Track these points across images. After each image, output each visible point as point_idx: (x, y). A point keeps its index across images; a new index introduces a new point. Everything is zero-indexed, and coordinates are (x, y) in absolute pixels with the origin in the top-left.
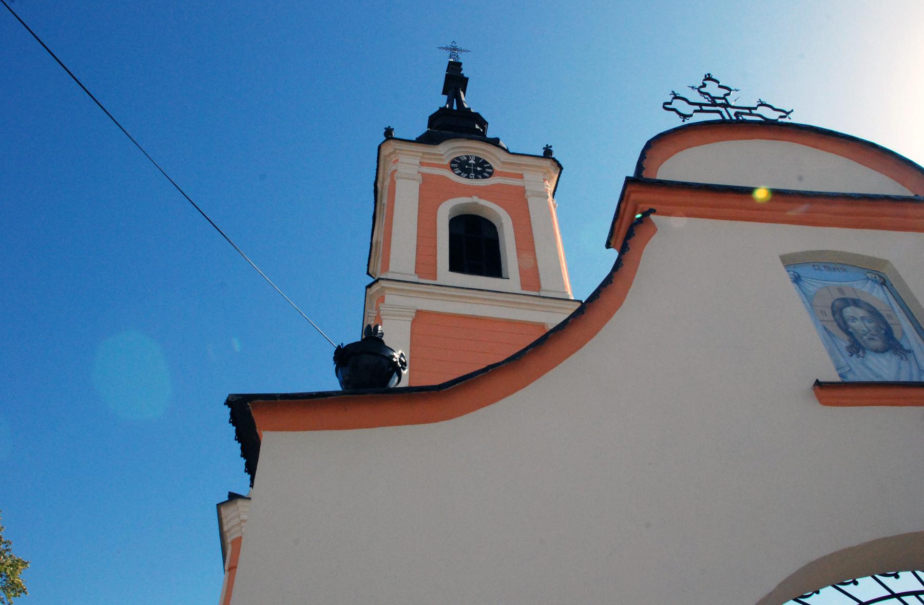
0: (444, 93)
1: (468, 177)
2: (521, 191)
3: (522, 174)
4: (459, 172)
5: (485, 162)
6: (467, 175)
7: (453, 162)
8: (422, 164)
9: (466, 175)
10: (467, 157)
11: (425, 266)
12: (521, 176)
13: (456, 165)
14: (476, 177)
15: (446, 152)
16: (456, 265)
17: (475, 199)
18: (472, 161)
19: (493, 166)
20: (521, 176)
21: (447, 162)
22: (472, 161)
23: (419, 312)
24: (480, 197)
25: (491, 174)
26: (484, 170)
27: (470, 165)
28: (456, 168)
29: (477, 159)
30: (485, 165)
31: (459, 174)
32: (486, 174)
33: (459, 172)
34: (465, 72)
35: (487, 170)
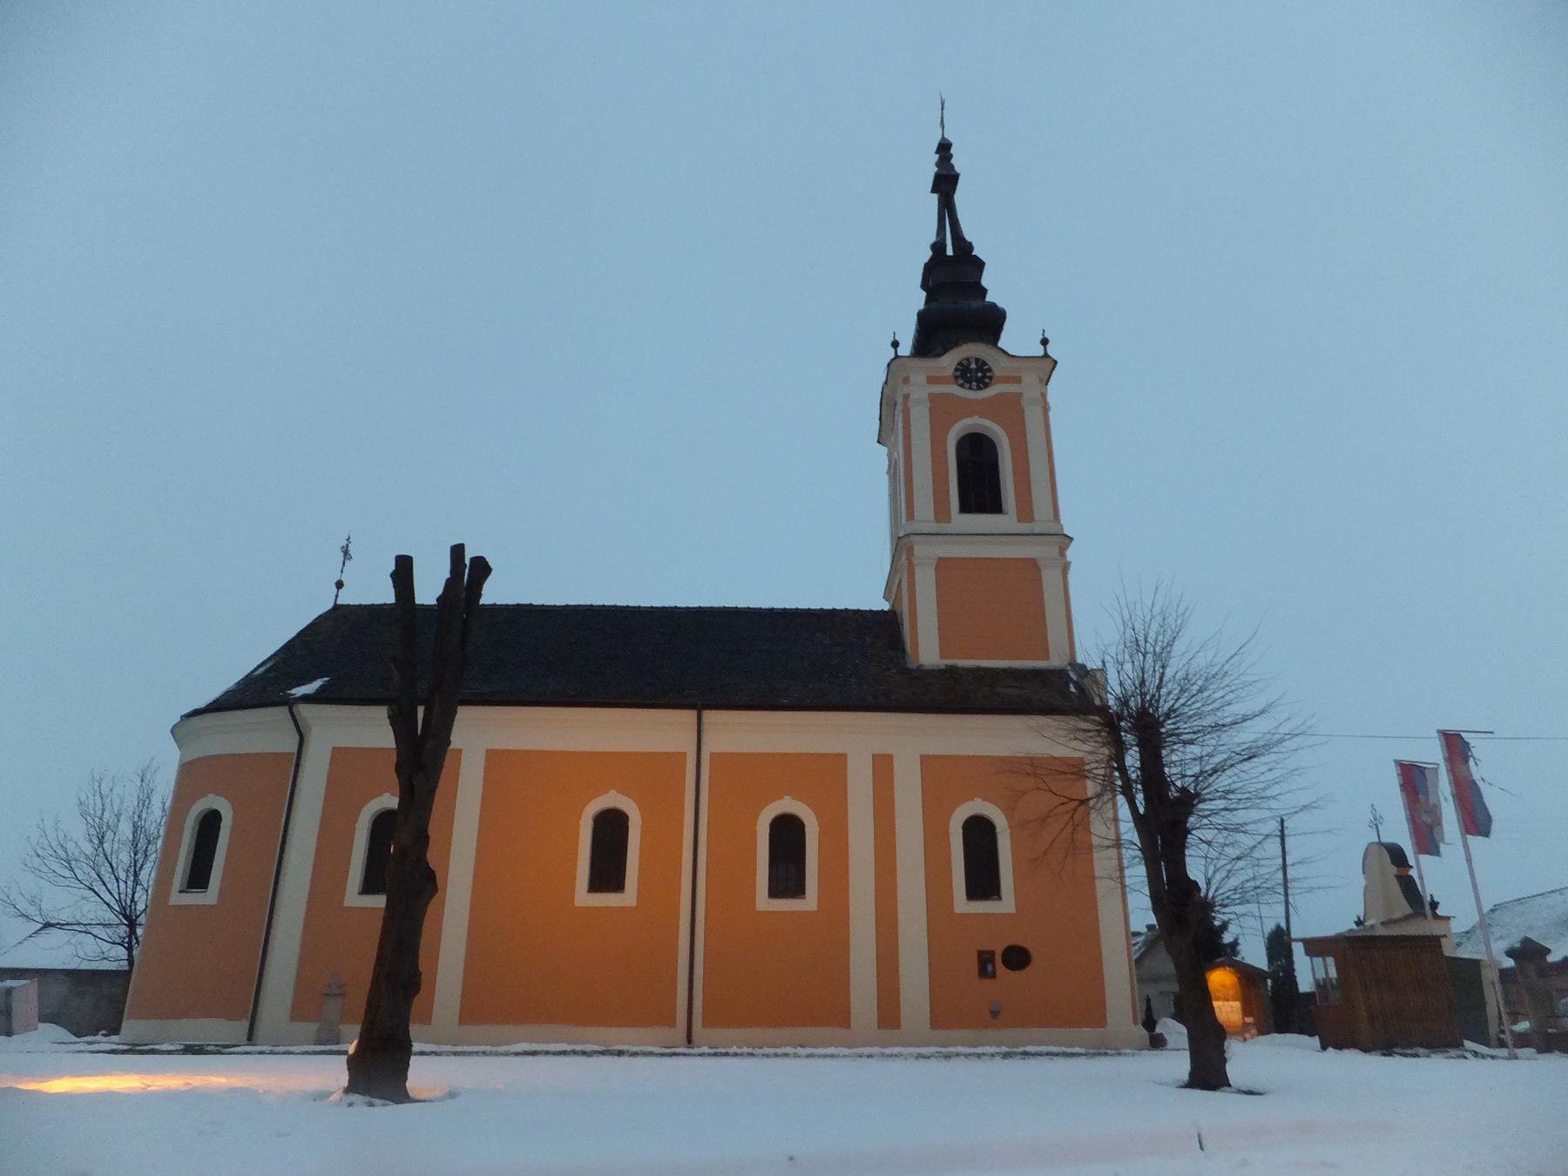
0: (933, 191)
1: (970, 388)
2: (1019, 396)
4: (961, 382)
7: (956, 370)
9: (967, 385)
10: (968, 359)
11: (942, 513)
13: (958, 373)
14: (979, 388)
16: (965, 508)
18: (973, 366)
20: (1017, 380)
21: (950, 372)
22: (973, 366)
23: (940, 559)
26: (984, 376)
27: (970, 371)
29: (977, 360)
30: (986, 367)
31: (962, 386)
32: (987, 380)
34: (957, 162)
35: (988, 374)
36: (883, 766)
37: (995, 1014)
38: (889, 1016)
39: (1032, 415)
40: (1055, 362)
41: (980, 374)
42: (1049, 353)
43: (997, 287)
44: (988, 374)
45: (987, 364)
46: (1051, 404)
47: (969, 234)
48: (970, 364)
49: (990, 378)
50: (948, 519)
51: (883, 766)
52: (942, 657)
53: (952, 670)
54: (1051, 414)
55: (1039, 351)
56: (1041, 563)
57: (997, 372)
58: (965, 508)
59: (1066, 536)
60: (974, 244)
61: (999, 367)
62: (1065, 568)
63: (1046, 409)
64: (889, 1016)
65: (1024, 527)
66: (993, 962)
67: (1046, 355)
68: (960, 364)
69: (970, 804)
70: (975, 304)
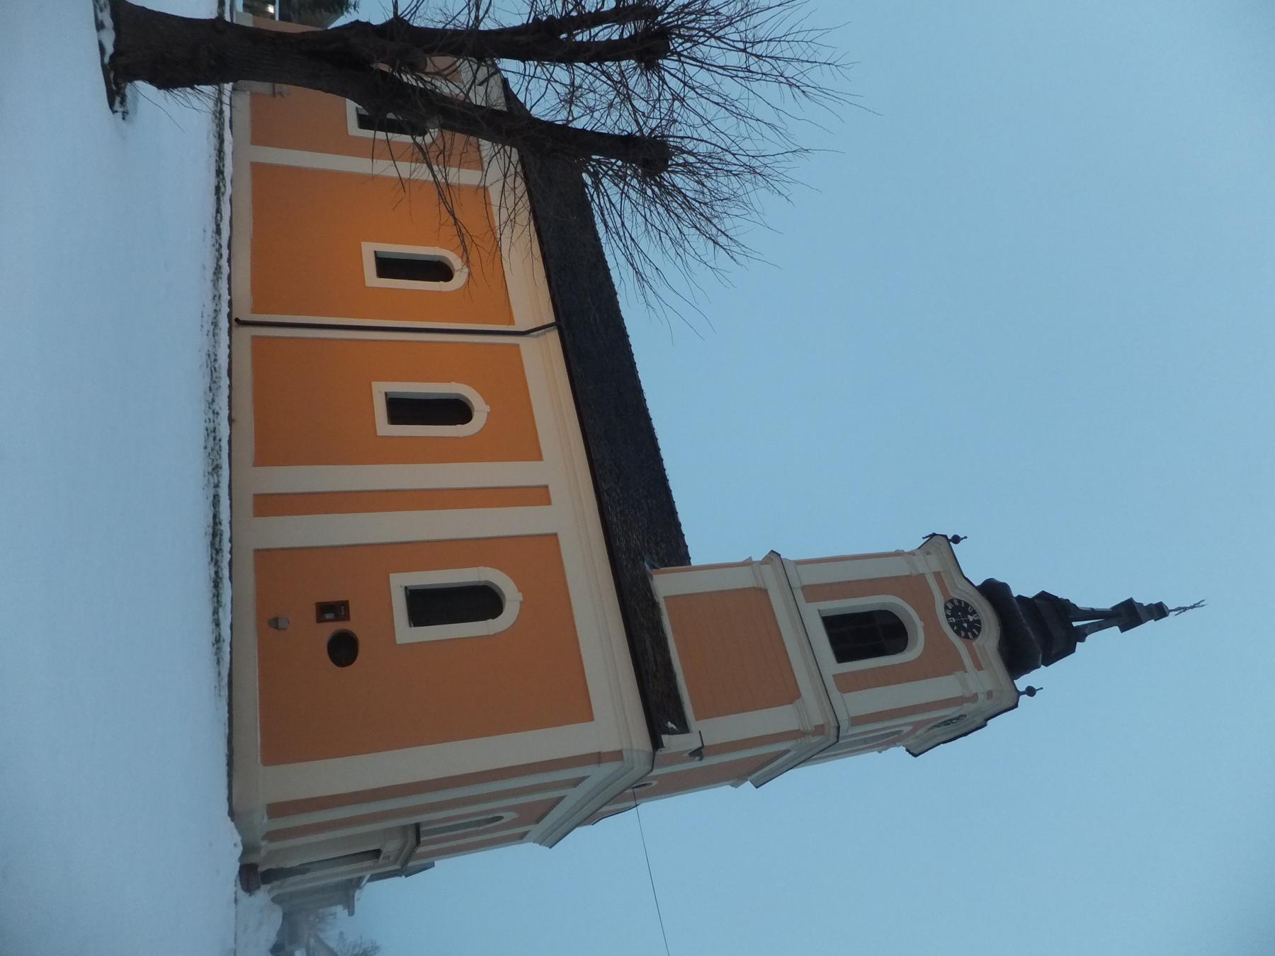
1: (948, 616)
4: (950, 607)
5: (979, 630)
6: (950, 614)
8: (937, 575)
9: (950, 614)
14: (952, 625)
15: (962, 590)
17: (920, 624)
18: (971, 618)
21: (955, 595)
22: (971, 618)
23: (766, 591)
24: (926, 629)
25: (967, 637)
26: (966, 630)
28: (953, 603)
31: (946, 608)
33: (950, 607)
35: (969, 634)
36: (539, 495)
38: (268, 505)
41: (965, 625)
42: (1022, 698)
44: (969, 634)
45: (979, 631)
48: (971, 615)
51: (539, 495)
64: (268, 505)
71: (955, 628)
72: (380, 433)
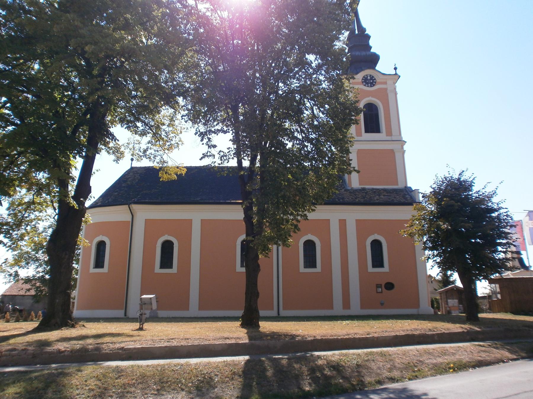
1: (368, 86)
2: (386, 89)
3: (386, 82)
5: (373, 77)
7: (362, 79)
10: (367, 75)
12: (385, 83)
13: (363, 81)
14: (371, 86)
16: (367, 131)
18: (369, 78)
19: (376, 79)
20: (385, 83)
21: (360, 80)
22: (369, 78)
23: (358, 150)
26: (373, 82)
27: (368, 80)
29: (370, 76)
31: (365, 85)
32: (374, 83)
35: (375, 81)
36: (343, 223)
37: (382, 304)
39: (391, 96)
40: (400, 76)
41: (371, 81)
42: (398, 72)
43: (375, 46)
44: (375, 81)
46: (398, 92)
47: (364, 24)
49: (375, 82)
50: (361, 135)
51: (343, 223)
52: (360, 185)
53: (364, 189)
54: (398, 96)
55: (393, 72)
56: (395, 151)
57: (378, 80)
58: (367, 131)
59: (404, 141)
60: (366, 29)
61: (379, 78)
62: (404, 152)
63: (396, 94)
65: (389, 138)
66: (381, 287)
67: (396, 74)
68: (364, 77)
69: (373, 236)
70: (368, 53)
71: (372, 85)
72: (176, 272)
